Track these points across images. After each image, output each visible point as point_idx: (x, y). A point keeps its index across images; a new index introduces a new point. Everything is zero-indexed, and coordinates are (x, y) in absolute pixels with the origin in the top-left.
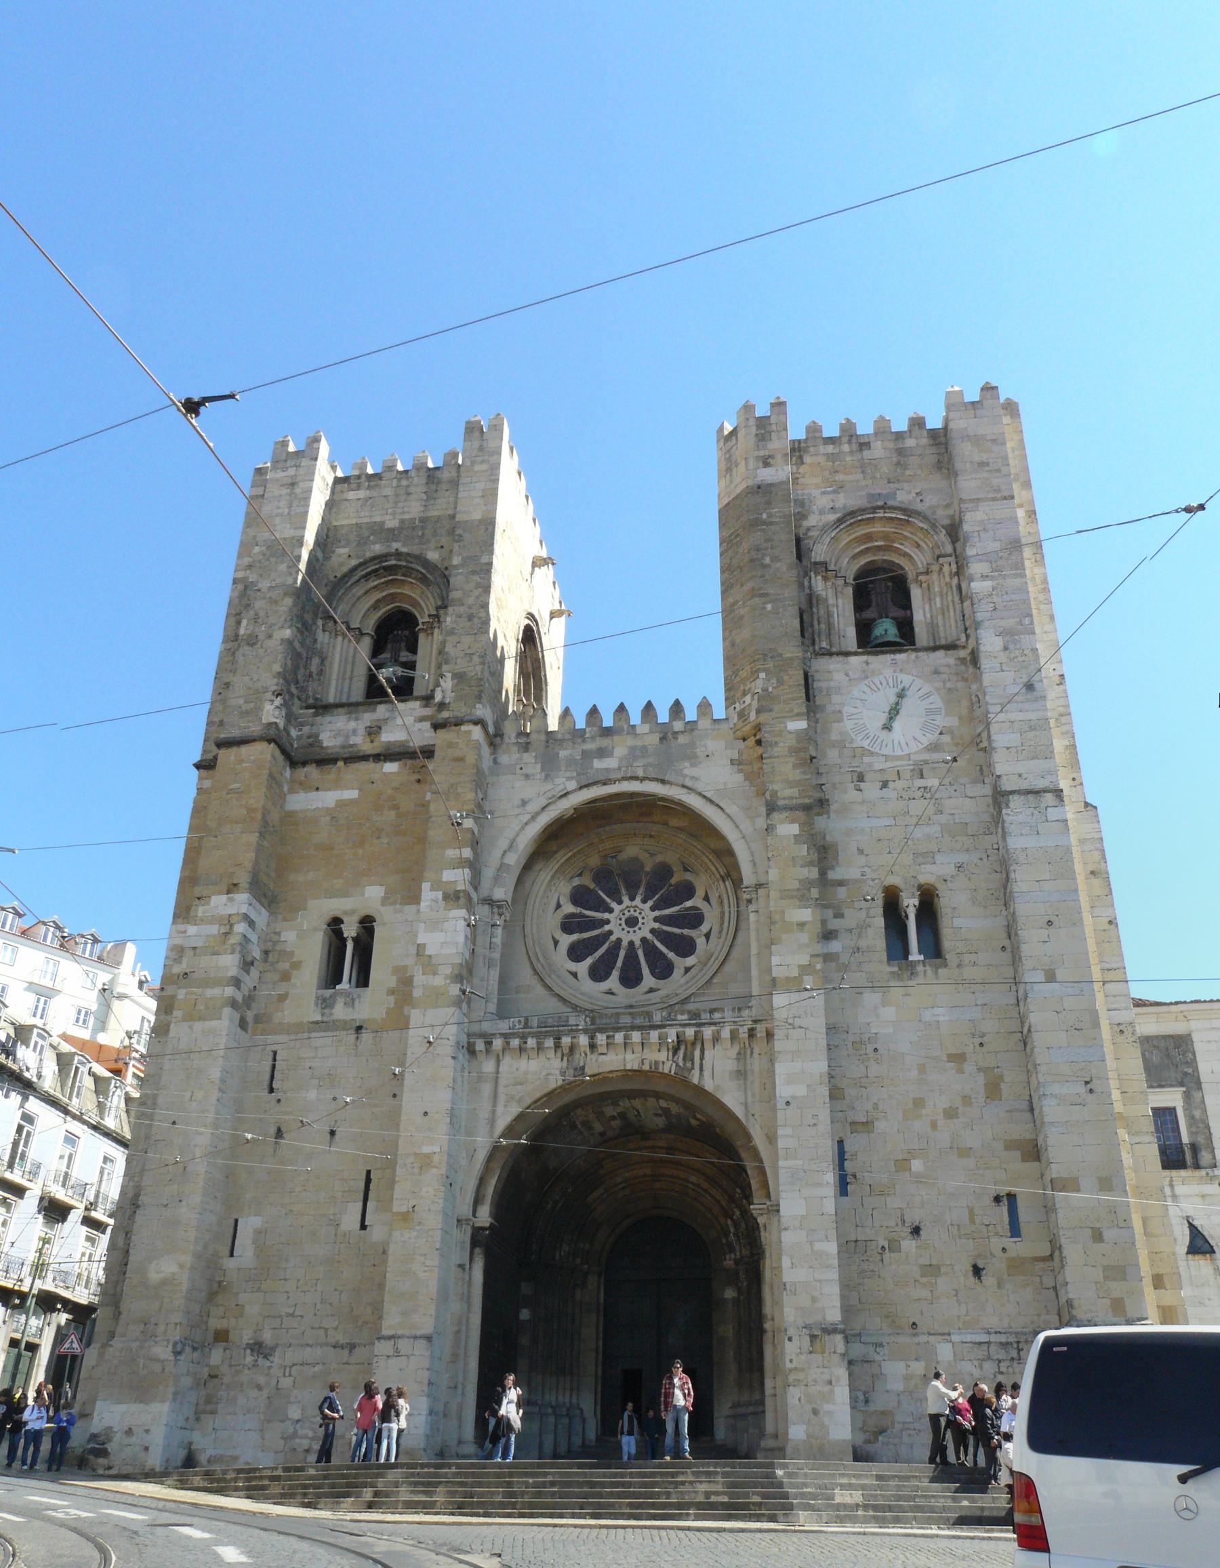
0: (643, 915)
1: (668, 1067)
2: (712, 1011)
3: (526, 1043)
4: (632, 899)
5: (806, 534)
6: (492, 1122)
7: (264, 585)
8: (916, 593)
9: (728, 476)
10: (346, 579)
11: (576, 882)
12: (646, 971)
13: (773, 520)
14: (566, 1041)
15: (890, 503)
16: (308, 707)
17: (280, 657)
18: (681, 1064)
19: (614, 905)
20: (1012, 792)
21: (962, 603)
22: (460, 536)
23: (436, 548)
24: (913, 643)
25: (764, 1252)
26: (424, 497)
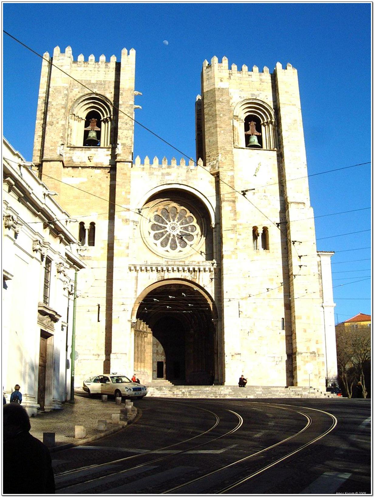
0: (177, 226)
1: (189, 278)
2: (203, 262)
3: (146, 268)
4: (174, 221)
5: (231, 105)
6: (136, 291)
7: (54, 103)
8: (263, 128)
9: (208, 81)
10: (78, 100)
11: (156, 213)
12: (178, 245)
13: (223, 101)
14: (159, 269)
15: (258, 98)
16: (68, 147)
17: (62, 131)
18: (193, 277)
19: (168, 222)
20: (292, 203)
21: (278, 136)
22: (122, 93)
23: (109, 93)
24: (262, 147)
25: (215, 332)
26: (104, 73)
